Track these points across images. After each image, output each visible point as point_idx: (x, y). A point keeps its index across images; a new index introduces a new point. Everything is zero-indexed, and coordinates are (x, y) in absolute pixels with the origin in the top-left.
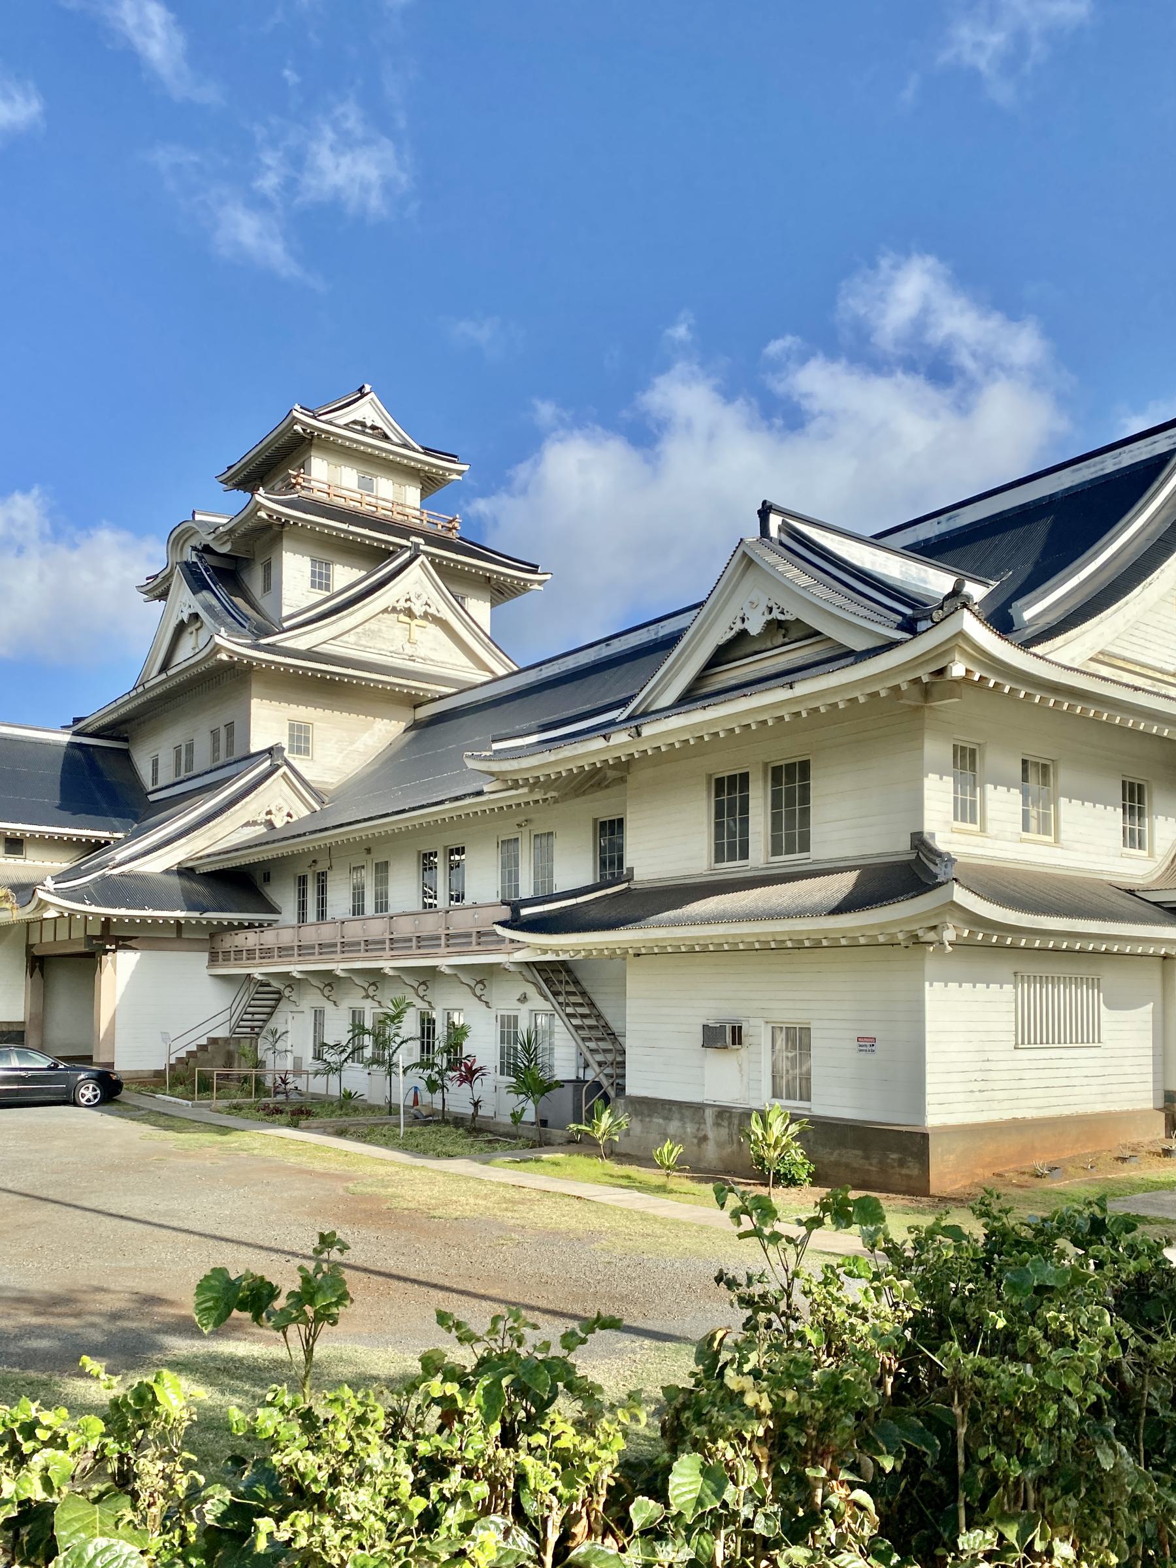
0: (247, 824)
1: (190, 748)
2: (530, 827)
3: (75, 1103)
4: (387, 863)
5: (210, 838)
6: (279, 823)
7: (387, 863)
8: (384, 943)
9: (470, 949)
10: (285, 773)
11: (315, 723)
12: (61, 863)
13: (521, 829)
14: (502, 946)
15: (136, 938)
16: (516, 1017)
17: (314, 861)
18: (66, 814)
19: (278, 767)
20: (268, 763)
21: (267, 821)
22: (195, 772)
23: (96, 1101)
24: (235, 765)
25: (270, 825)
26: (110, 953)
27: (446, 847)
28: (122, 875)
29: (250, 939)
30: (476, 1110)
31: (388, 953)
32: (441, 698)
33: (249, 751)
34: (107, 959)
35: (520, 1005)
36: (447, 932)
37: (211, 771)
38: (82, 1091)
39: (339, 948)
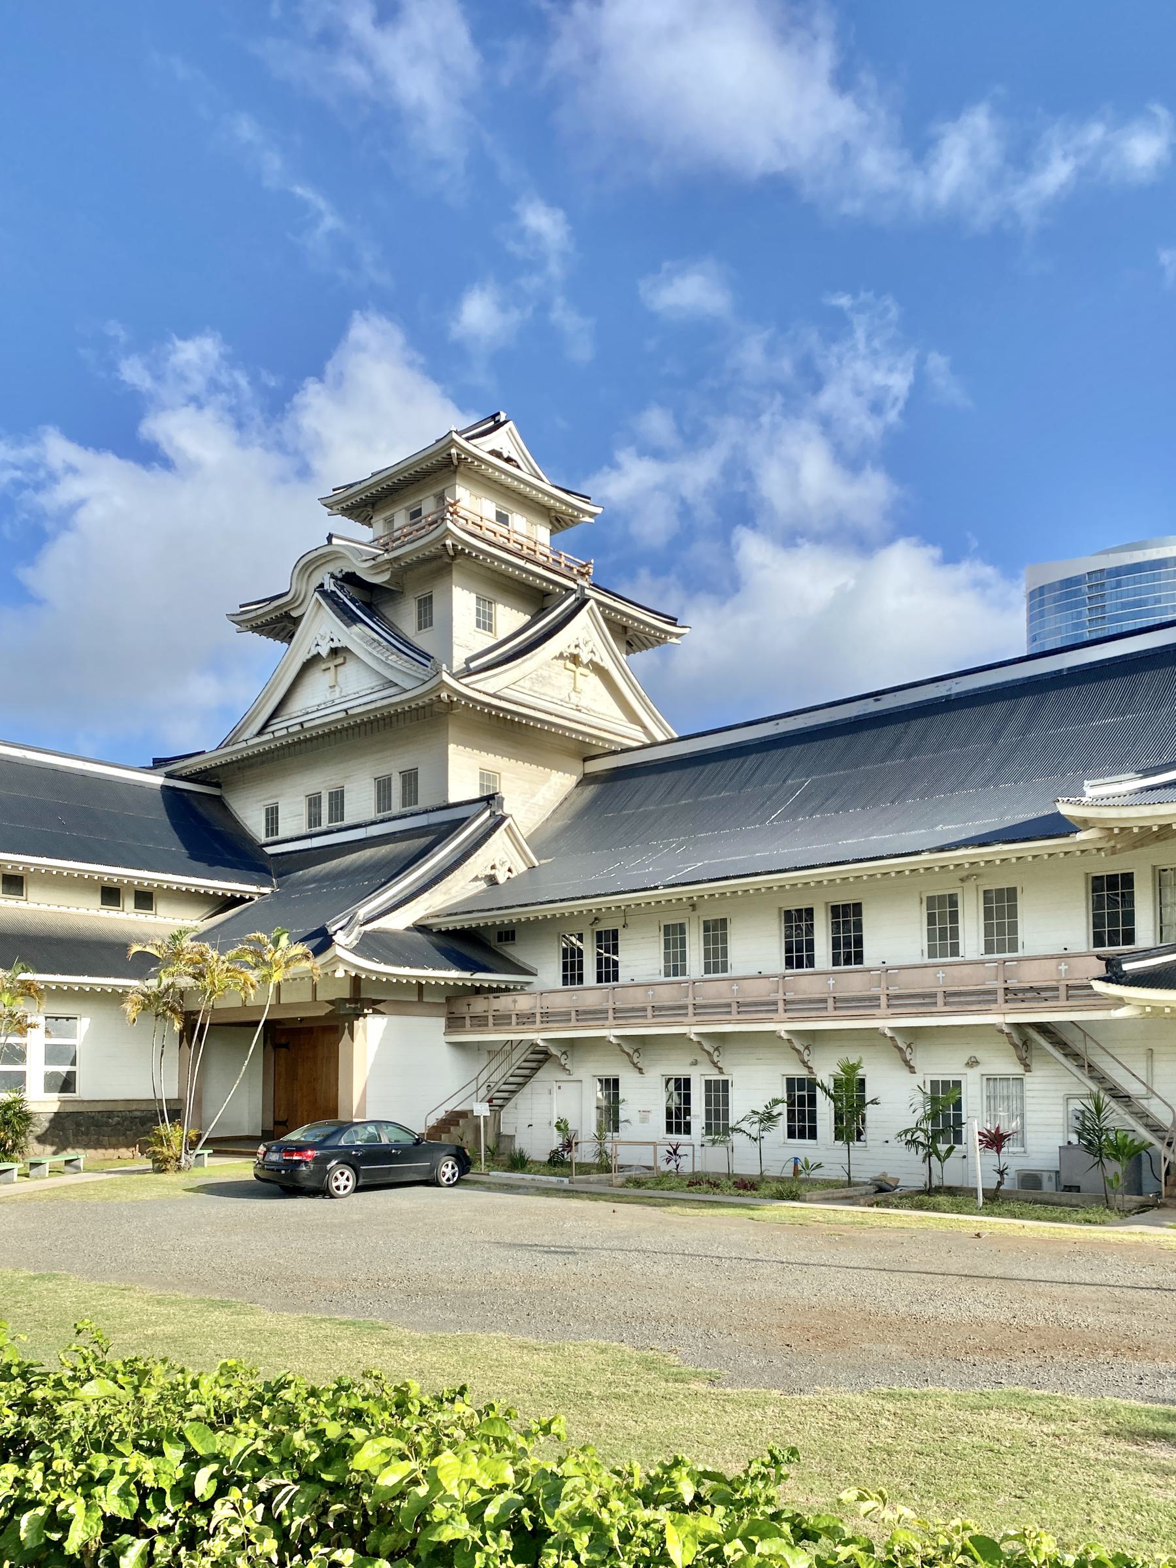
0: (473, 880)
1: (337, 799)
2: (979, 882)
3: (436, 1184)
4: (724, 921)
5: (445, 893)
6: (501, 879)
7: (724, 921)
8: (775, 1003)
9: (934, 1009)
10: (509, 826)
11: (503, 774)
12: (193, 920)
13: (963, 885)
14: (993, 1006)
15: (384, 1001)
16: (958, 1084)
17: (596, 919)
18: (201, 866)
19: (503, 819)
20: (487, 813)
21: (486, 876)
22: (348, 821)
23: (455, 1179)
24: (425, 816)
25: (492, 880)
26: (361, 1019)
27: (827, 903)
28: (374, 931)
29: (523, 1003)
30: (1002, 1178)
31: (782, 1015)
32: (623, 751)
33: (446, 800)
34: (359, 1024)
35: (968, 1071)
36: (888, 992)
37: (382, 821)
38: (443, 1169)
39: (691, 1010)
